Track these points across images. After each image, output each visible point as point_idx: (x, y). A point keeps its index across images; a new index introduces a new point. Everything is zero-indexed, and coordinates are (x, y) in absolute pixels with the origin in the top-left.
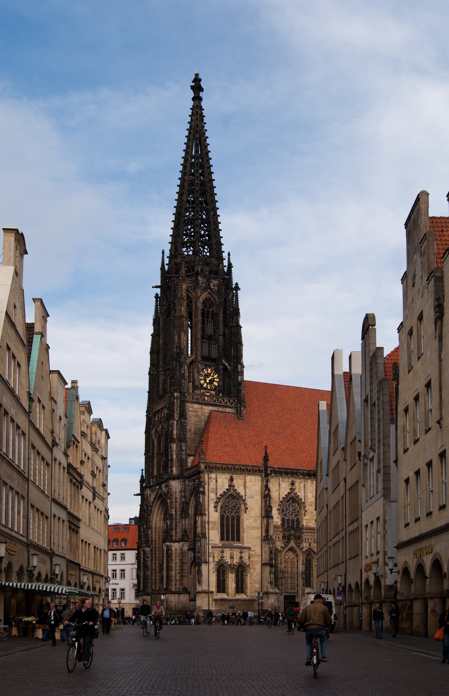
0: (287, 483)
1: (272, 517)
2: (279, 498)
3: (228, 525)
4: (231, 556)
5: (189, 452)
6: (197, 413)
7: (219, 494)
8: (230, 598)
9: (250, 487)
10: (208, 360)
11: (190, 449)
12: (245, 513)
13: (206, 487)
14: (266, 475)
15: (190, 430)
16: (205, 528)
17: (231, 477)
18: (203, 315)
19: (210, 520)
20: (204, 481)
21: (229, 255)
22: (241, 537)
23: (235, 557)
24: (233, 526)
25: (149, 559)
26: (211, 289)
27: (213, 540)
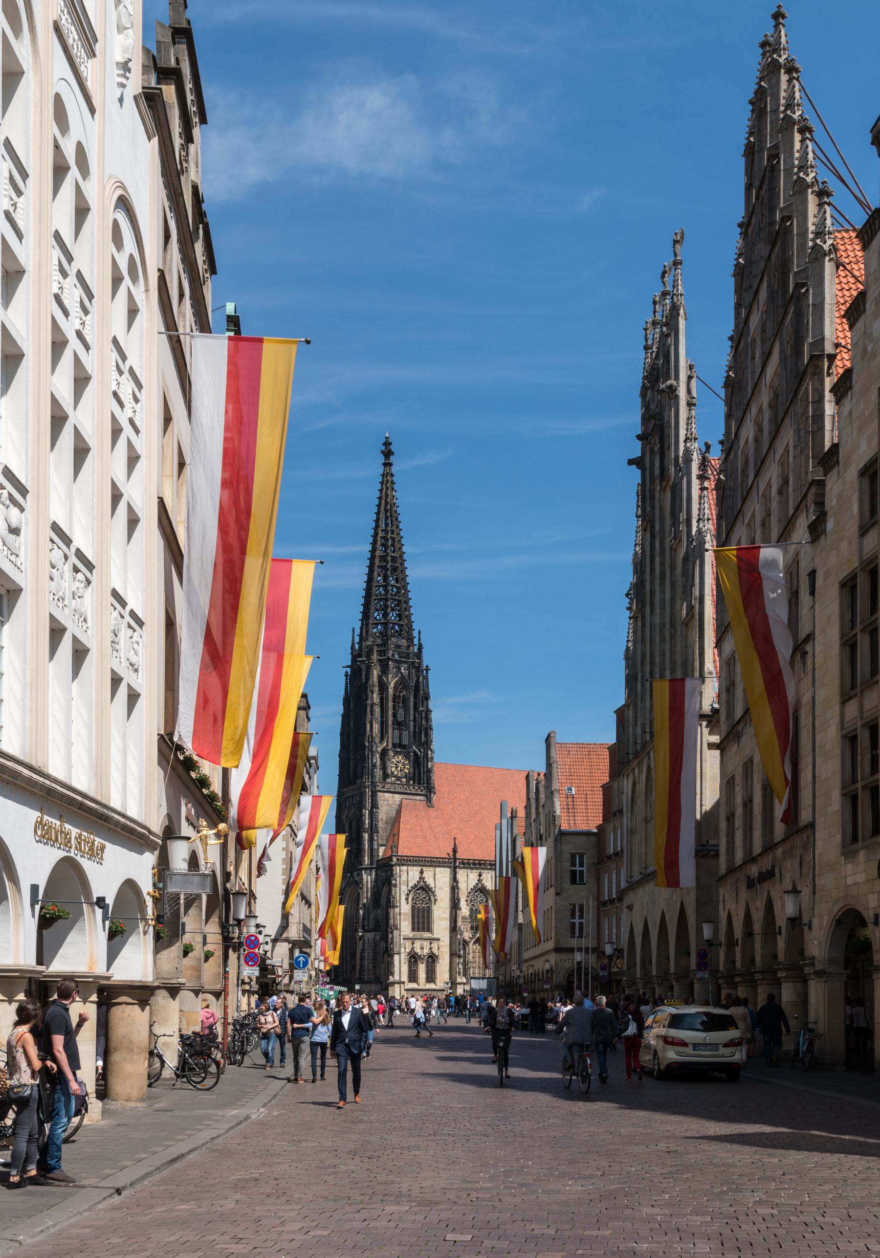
1: (460, 909)
3: (418, 916)
4: (422, 948)
5: (380, 842)
6: (388, 802)
7: (410, 886)
8: (420, 987)
9: (439, 879)
10: (399, 746)
14: (455, 868)
18: (394, 701)
21: (420, 633)
24: (423, 917)
26: (402, 674)
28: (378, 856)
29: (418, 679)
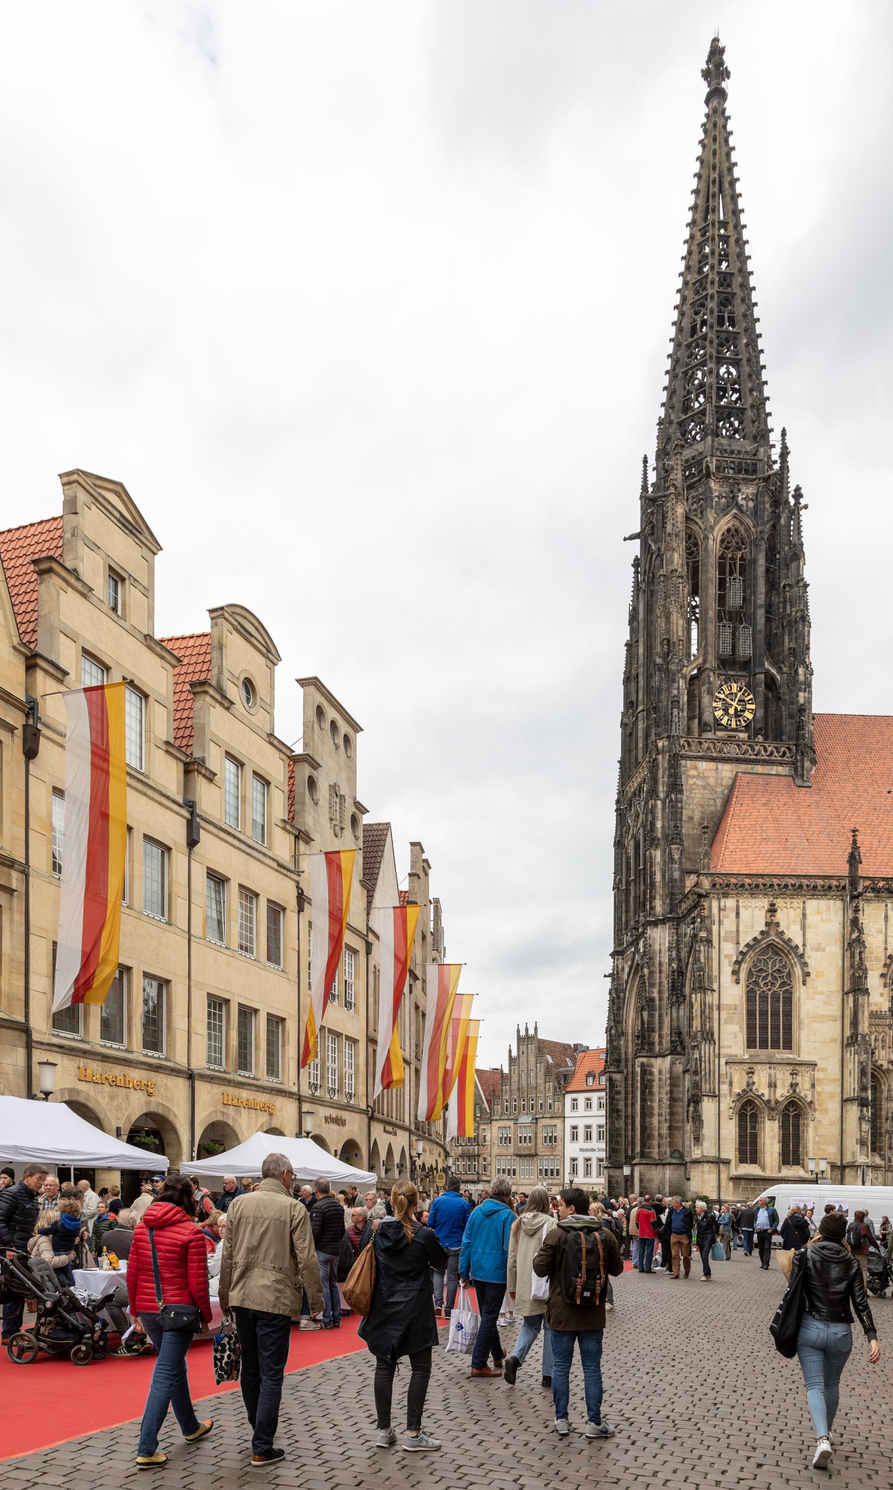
3: (764, 1014)
12: (804, 984)
13: (715, 928)
16: (711, 1019)
17: (772, 905)
19: (722, 1002)
20: (710, 917)
22: (794, 1040)
23: (779, 1084)
24: (775, 1014)
27: (730, 1047)
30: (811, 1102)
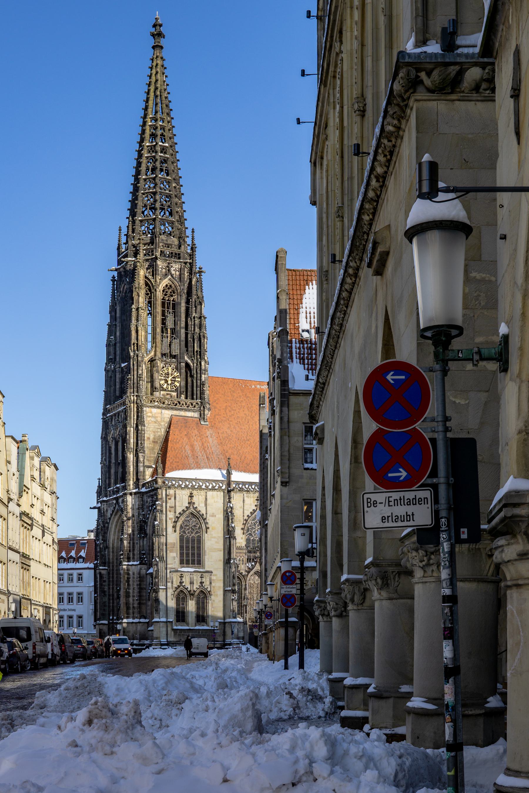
0: (252, 499)
1: (235, 538)
2: (244, 516)
5: (147, 463)
6: (155, 419)
7: (177, 513)
11: (148, 460)
14: (229, 492)
15: (149, 438)
21: (193, 231)
23: (195, 582)
24: (193, 547)
25: (107, 583)
28: (144, 479)
29: (191, 280)
30: (210, 591)
